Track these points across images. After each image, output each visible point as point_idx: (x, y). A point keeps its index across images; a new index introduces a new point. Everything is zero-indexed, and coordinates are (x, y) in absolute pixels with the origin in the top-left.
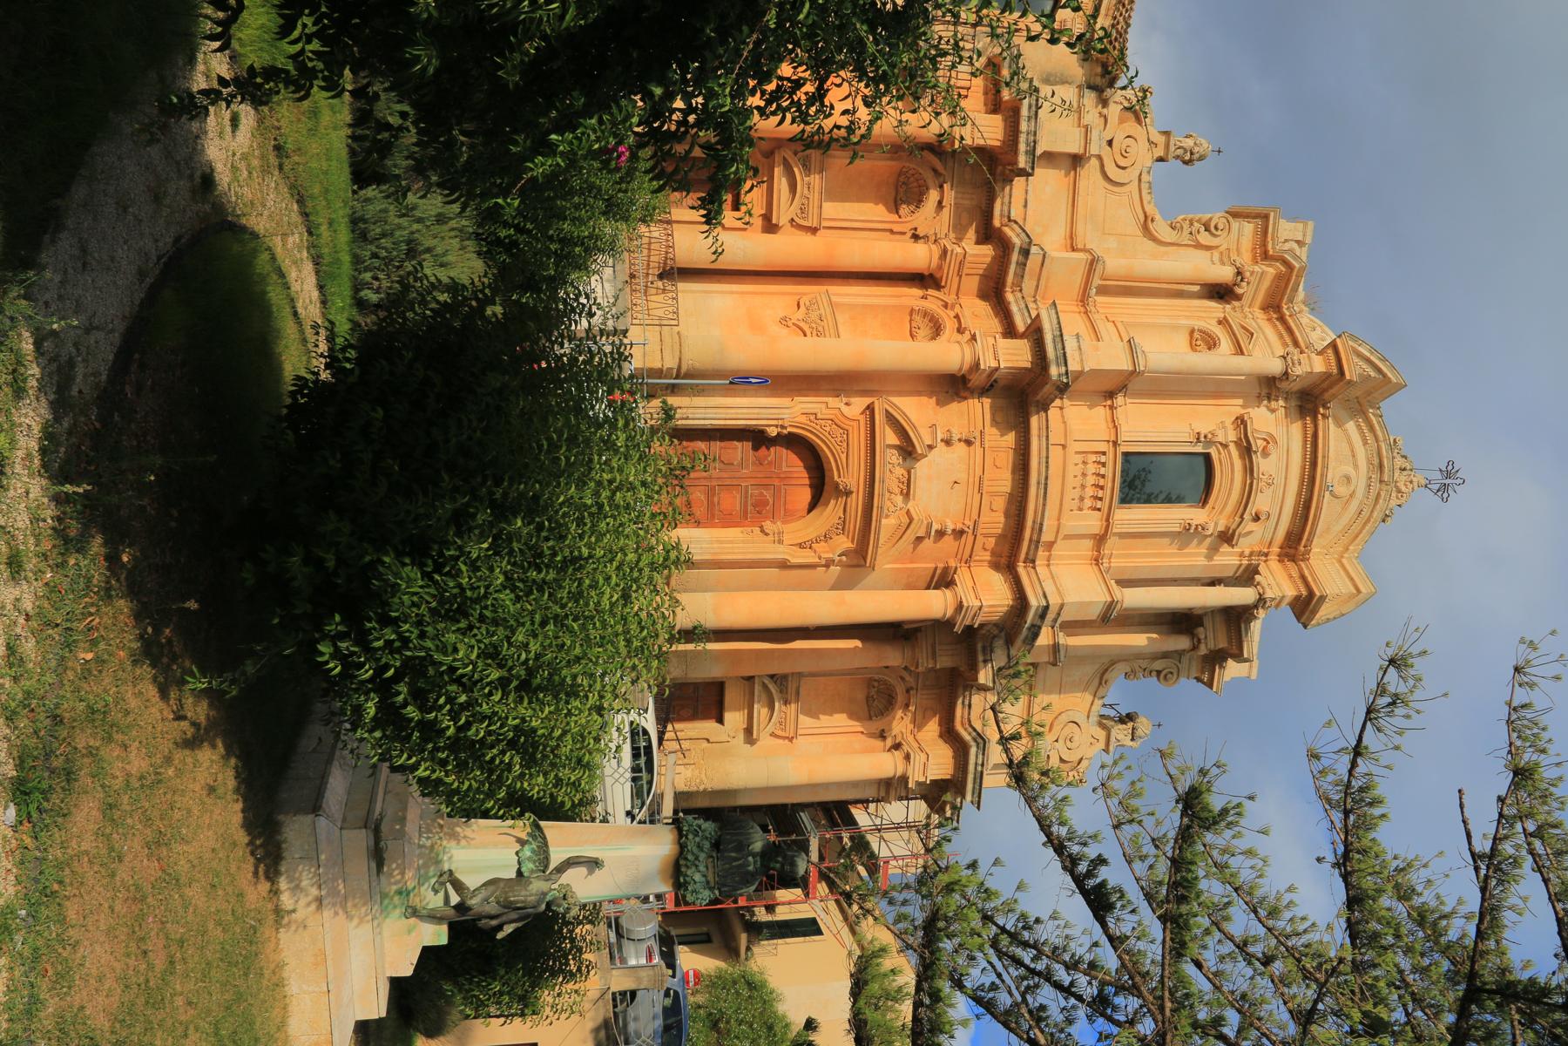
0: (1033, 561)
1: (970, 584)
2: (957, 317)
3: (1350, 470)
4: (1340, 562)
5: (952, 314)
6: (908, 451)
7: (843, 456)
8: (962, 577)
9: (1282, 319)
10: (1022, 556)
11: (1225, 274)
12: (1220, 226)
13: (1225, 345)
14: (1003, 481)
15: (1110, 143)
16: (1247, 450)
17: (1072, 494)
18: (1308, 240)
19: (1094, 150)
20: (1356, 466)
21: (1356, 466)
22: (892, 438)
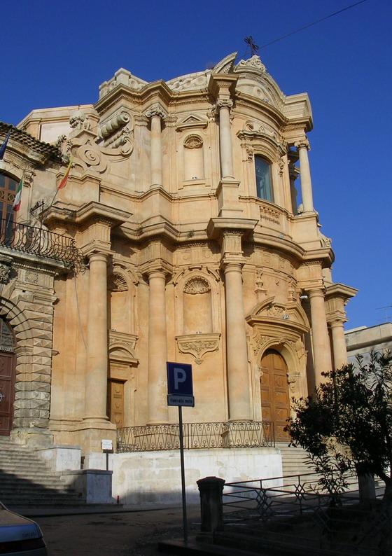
0: (304, 251)
1: (309, 283)
2: (191, 270)
3: (255, 89)
4: (286, 105)
5: (187, 272)
6: (269, 306)
7: (271, 338)
8: (306, 286)
9: (178, 99)
10: (301, 255)
11: (156, 122)
12: (126, 117)
13: (197, 132)
14: (275, 259)
15: (89, 165)
16: (255, 136)
17: (275, 226)
18: (129, 73)
19: (97, 175)
20: (253, 86)
21: (253, 86)
22: (264, 313)
